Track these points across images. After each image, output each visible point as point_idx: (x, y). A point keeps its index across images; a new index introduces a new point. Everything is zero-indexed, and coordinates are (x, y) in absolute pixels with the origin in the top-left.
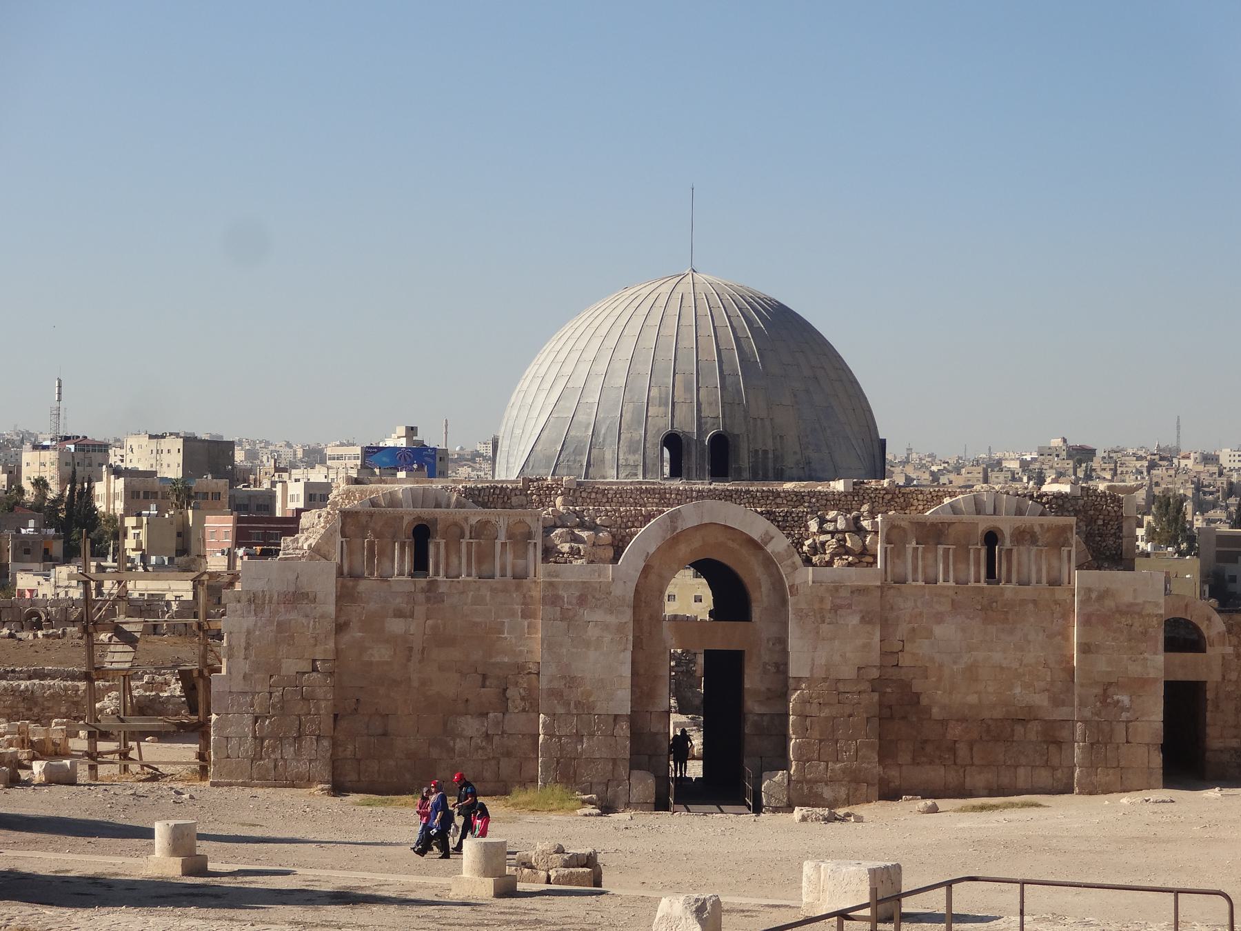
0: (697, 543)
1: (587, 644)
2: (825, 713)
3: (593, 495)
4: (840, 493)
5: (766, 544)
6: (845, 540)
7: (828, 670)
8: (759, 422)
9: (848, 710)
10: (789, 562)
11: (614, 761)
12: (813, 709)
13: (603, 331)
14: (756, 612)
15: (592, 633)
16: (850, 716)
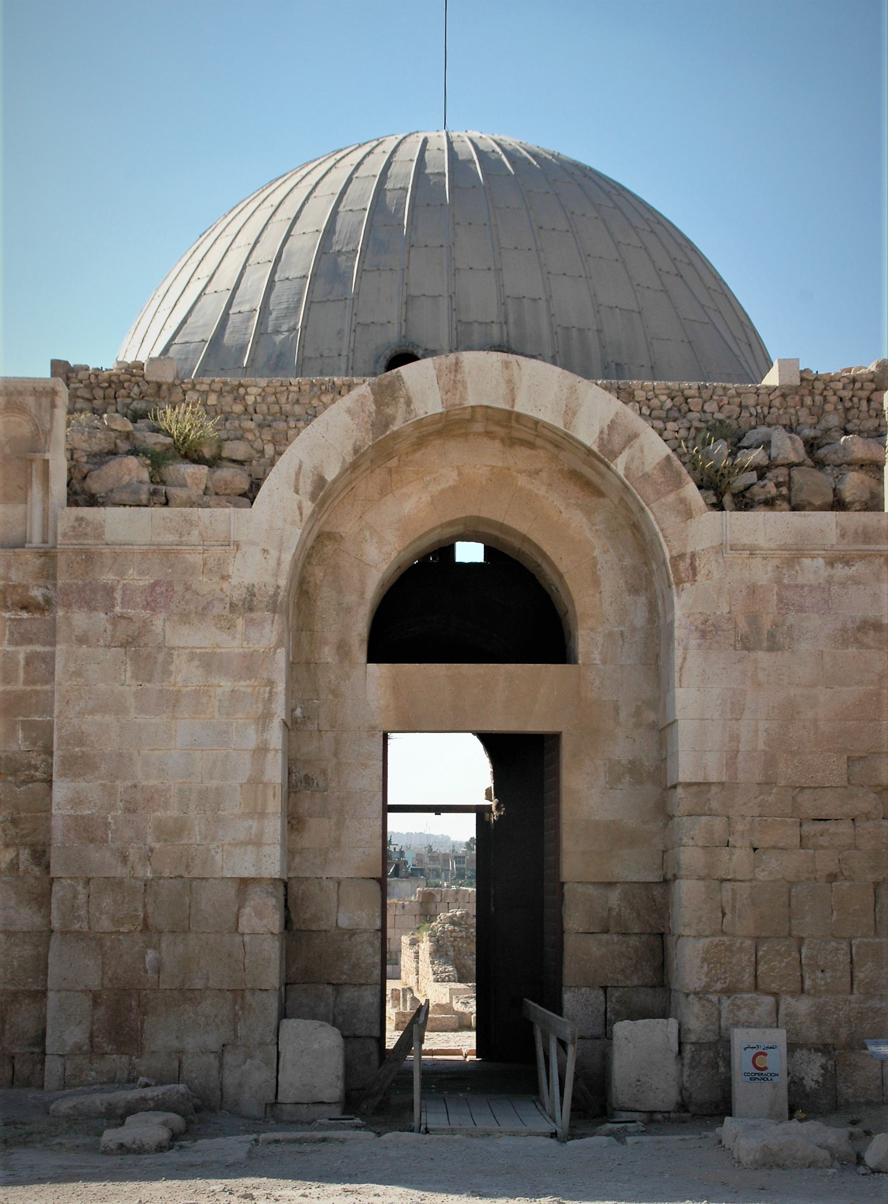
0: (450, 478)
1: (171, 701)
2: (774, 867)
3: (212, 399)
4: (771, 390)
5: (614, 455)
6: (789, 483)
7: (770, 762)
8: (574, 333)
9: (826, 862)
10: (671, 498)
11: (238, 994)
12: (737, 860)
13: (275, 199)
14: (587, 640)
15: (185, 675)
16: (832, 877)
